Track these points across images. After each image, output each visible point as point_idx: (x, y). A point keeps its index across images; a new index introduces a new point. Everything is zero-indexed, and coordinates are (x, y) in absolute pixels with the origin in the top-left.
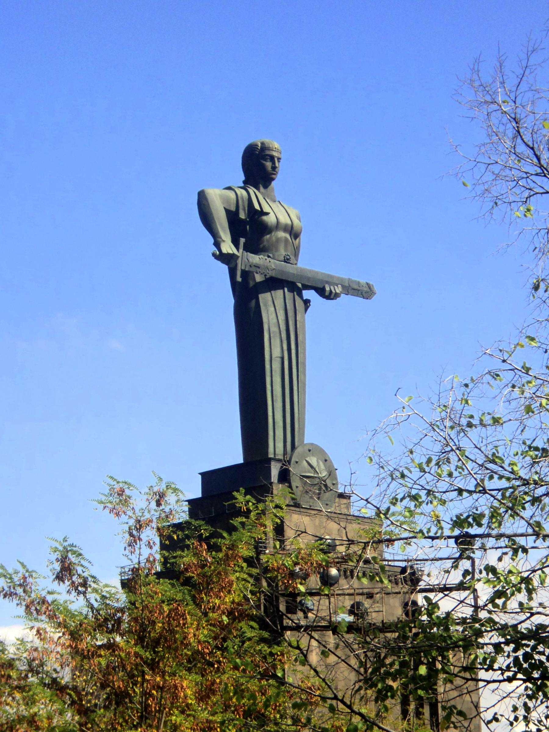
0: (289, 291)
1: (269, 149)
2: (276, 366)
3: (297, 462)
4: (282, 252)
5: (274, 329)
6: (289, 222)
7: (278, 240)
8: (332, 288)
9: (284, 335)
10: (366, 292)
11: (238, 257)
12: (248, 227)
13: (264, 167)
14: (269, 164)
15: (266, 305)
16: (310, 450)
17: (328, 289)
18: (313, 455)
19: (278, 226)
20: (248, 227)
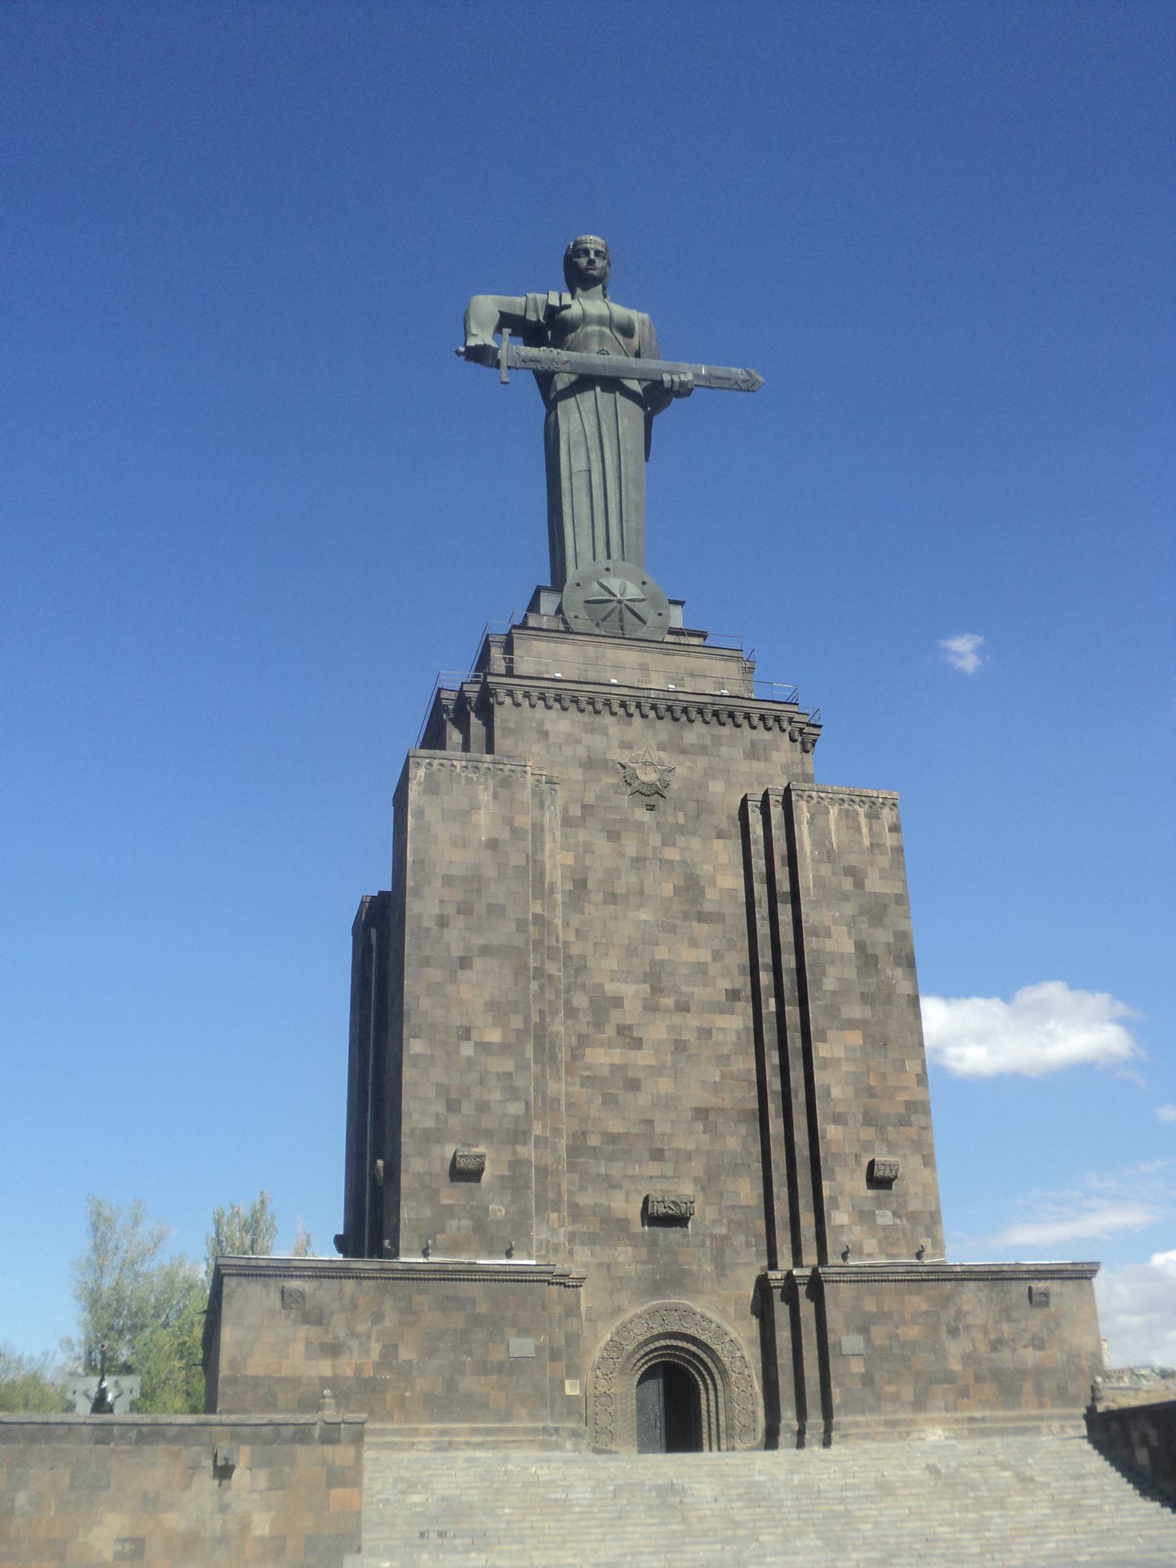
0: (602, 390)
1: (581, 242)
2: (580, 482)
3: (578, 585)
4: (595, 346)
5: (576, 437)
6: (605, 312)
7: (587, 336)
8: (676, 378)
9: (593, 443)
11: (496, 351)
12: (549, 333)
13: (576, 265)
14: (583, 261)
15: (566, 413)
16: (608, 570)
17: (666, 378)
18: (615, 576)
19: (585, 319)
20: (549, 333)
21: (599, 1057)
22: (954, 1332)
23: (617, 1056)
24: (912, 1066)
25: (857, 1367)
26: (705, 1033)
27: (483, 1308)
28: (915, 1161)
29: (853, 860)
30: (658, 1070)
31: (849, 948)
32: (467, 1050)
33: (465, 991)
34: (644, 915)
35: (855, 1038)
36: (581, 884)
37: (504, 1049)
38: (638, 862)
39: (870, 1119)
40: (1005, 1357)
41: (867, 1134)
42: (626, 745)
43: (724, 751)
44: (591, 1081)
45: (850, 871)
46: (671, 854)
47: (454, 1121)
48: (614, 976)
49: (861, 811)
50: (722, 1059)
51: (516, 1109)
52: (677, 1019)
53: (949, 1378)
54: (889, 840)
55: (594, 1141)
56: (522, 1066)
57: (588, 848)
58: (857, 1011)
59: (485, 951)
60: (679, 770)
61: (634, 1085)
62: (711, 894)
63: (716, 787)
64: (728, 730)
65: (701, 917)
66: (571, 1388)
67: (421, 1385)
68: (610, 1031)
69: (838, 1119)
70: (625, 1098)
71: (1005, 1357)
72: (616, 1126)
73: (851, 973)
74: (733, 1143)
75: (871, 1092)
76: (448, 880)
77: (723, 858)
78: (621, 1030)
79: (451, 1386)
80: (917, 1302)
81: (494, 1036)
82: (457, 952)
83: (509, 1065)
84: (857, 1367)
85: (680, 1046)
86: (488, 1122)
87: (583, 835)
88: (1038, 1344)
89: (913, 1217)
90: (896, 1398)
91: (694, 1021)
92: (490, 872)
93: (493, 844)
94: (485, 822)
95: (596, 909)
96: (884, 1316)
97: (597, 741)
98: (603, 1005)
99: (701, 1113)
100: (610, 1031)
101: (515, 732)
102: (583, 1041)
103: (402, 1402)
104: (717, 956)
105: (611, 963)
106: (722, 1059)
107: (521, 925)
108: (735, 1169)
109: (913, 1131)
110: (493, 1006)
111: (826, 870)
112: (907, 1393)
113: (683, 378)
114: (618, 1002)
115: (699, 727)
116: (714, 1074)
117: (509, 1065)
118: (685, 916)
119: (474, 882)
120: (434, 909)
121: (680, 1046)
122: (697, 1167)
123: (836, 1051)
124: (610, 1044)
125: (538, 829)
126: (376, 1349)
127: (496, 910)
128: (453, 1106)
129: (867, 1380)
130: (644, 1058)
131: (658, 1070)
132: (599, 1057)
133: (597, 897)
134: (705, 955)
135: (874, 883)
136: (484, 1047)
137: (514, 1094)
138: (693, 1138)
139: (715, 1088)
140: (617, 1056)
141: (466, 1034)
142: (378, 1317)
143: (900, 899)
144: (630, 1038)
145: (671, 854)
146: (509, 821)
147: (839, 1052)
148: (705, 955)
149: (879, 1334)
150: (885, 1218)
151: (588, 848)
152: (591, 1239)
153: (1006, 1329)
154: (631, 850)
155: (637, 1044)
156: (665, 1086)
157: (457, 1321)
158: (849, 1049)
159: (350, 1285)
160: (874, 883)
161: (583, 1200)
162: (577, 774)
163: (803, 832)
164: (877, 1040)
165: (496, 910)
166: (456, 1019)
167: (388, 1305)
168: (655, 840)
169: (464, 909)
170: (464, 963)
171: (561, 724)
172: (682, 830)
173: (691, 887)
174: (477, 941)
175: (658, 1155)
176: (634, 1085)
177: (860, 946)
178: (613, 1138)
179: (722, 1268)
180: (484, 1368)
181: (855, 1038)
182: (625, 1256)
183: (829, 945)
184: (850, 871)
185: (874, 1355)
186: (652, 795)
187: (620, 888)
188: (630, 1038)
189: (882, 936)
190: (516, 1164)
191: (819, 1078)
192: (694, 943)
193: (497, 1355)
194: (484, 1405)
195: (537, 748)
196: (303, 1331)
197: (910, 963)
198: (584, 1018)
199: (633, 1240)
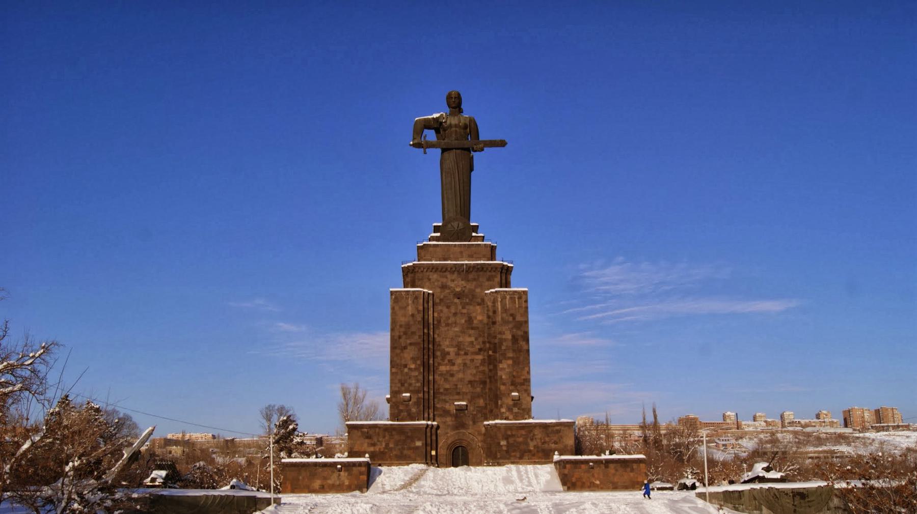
10: (502, 144)
21: (443, 368)
22: (532, 440)
23: (448, 368)
24: (527, 369)
25: (504, 448)
26: (472, 360)
27: (409, 434)
28: (525, 395)
29: (512, 312)
30: (459, 371)
31: (510, 337)
32: (406, 370)
33: (406, 355)
34: (457, 329)
35: (510, 362)
36: (439, 322)
37: (415, 369)
38: (455, 314)
39: (513, 384)
40: (546, 446)
41: (512, 388)
42: (453, 281)
43: (481, 279)
44: (441, 375)
45: (512, 315)
46: (465, 311)
47: (403, 389)
48: (448, 347)
49: (516, 297)
50: (477, 367)
51: (418, 385)
52: (465, 357)
53: (530, 451)
54: (524, 305)
55: (442, 390)
56: (420, 373)
57: (441, 311)
58: (510, 355)
59: (411, 344)
60: (468, 287)
61: (452, 375)
62: (475, 322)
63: (478, 290)
64: (481, 273)
65: (472, 328)
66: (433, 453)
67: (394, 453)
68: (446, 361)
69: (504, 384)
70: (451, 379)
71: (546, 446)
72: (447, 386)
73: (510, 344)
74: (478, 390)
75: (514, 376)
76: (401, 326)
77: (479, 311)
78: (449, 361)
79: (402, 453)
80: (523, 432)
81: (413, 366)
82: (403, 345)
83: (417, 374)
84: (504, 448)
85: (465, 364)
86: (411, 388)
87: (440, 308)
88: (556, 443)
89: (523, 410)
90: (515, 456)
91: (469, 357)
92: (412, 323)
93: (413, 315)
94: (410, 309)
95: (443, 329)
96: (513, 436)
97: (444, 280)
98: (445, 354)
99: (470, 382)
100: (446, 361)
101: (422, 279)
102: (439, 364)
103: (390, 457)
104: (476, 339)
105: (447, 343)
106: (477, 367)
107: (420, 336)
108: (479, 397)
109: (525, 387)
110: (412, 358)
111: (504, 315)
112: (518, 455)
113: (481, 146)
114: (448, 353)
115: (474, 273)
116: (475, 371)
117: (417, 374)
118: (468, 328)
119: (408, 326)
120: (397, 334)
121: (465, 364)
122: (469, 397)
123: (505, 368)
124: (446, 365)
125: (425, 311)
126: (384, 444)
127: (413, 333)
128: (403, 385)
129: (507, 452)
130: (455, 368)
131: (459, 371)
132: (443, 368)
133: (443, 325)
134: (473, 339)
135: (519, 318)
136: (410, 369)
137: (418, 381)
138: (466, 389)
139: (475, 375)
140: (448, 368)
141: (405, 366)
142: (384, 437)
143: (526, 322)
144: (452, 363)
145: (465, 311)
146: (417, 309)
147: (505, 366)
148: (473, 339)
149: (511, 440)
150: (516, 410)
151: (441, 311)
152: (440, 416)
153: (547, 439)
154: (453, 311)
155: (454, 364)
156: (461, 375)
157: (403, 438)
158: (509, 365)
159: (377, 430)
160: (519, 318)
161: (438, 406)
162: (438, 290)
163: (499, 305)
164: (516, 362)
165: (413, 333)
166: (403, 362)
167: (387, 434)
168: (460, 307)
169: (405, 333)
170: (405, 348)
171: (434, 276)
172: (468, 304)
173: (470, 320)
174: (408, 342)
175: (458, 394)
176: (452, 375)
177: (513, 336)
178: (446, 389)
179: (474, 423)
180: (410, 449)
181: (510, 362)
182: (449, 420)
183: (504, 337)
184: (512, 315)
185: (508, 445)
186: (459, 296)
187: (450, 321)
188: (452, 363)
189: (520, 333)
190: (418, 398)
191: (499, 373)
192: (470, 336)
193: (412, 446)
194: (409, 457)
195: (427, 284)
196: (367, 440)
197: (527, 341)
198: (439, 358)
199: (451, 415)
